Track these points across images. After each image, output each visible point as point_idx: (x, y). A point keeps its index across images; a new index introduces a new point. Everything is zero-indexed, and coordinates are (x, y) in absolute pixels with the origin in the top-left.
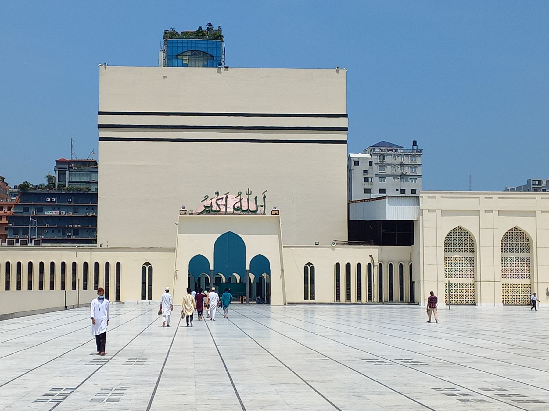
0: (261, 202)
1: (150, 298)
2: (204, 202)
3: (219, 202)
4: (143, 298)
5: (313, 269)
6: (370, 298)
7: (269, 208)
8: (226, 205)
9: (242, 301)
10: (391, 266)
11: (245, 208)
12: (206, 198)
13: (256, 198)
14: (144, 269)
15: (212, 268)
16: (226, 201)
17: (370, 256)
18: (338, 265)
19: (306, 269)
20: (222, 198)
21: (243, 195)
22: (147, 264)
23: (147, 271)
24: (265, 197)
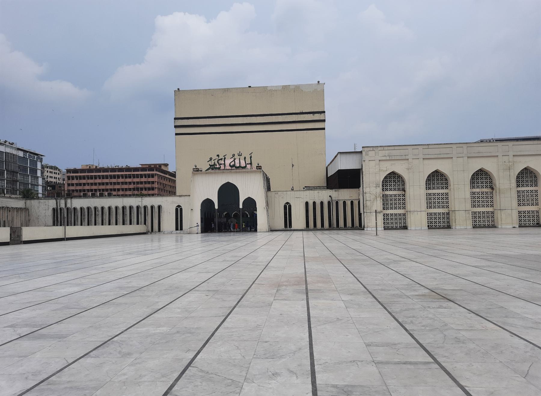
0: (248, 161)
1: (181, 229)
2: (210, 163)
3: (221, 162)
4: (177, 229)
5: (290, 206)
6: (330, 225)
7: (255, 165)
8: (225, 164)
9: (251, 229)
10: (344, 203)
11: (238, 165)
12: (211, 159)
13: (245, 158)
14: (177, 210)
15: (216, 207)
16: (224, 161)
17: (330, 196)
18: (307, 203)
19: (285, 207)
20: (222, 159)
21: (236, 156)
22: (179, 206)
23: (179, 211)
24: (251, 157)
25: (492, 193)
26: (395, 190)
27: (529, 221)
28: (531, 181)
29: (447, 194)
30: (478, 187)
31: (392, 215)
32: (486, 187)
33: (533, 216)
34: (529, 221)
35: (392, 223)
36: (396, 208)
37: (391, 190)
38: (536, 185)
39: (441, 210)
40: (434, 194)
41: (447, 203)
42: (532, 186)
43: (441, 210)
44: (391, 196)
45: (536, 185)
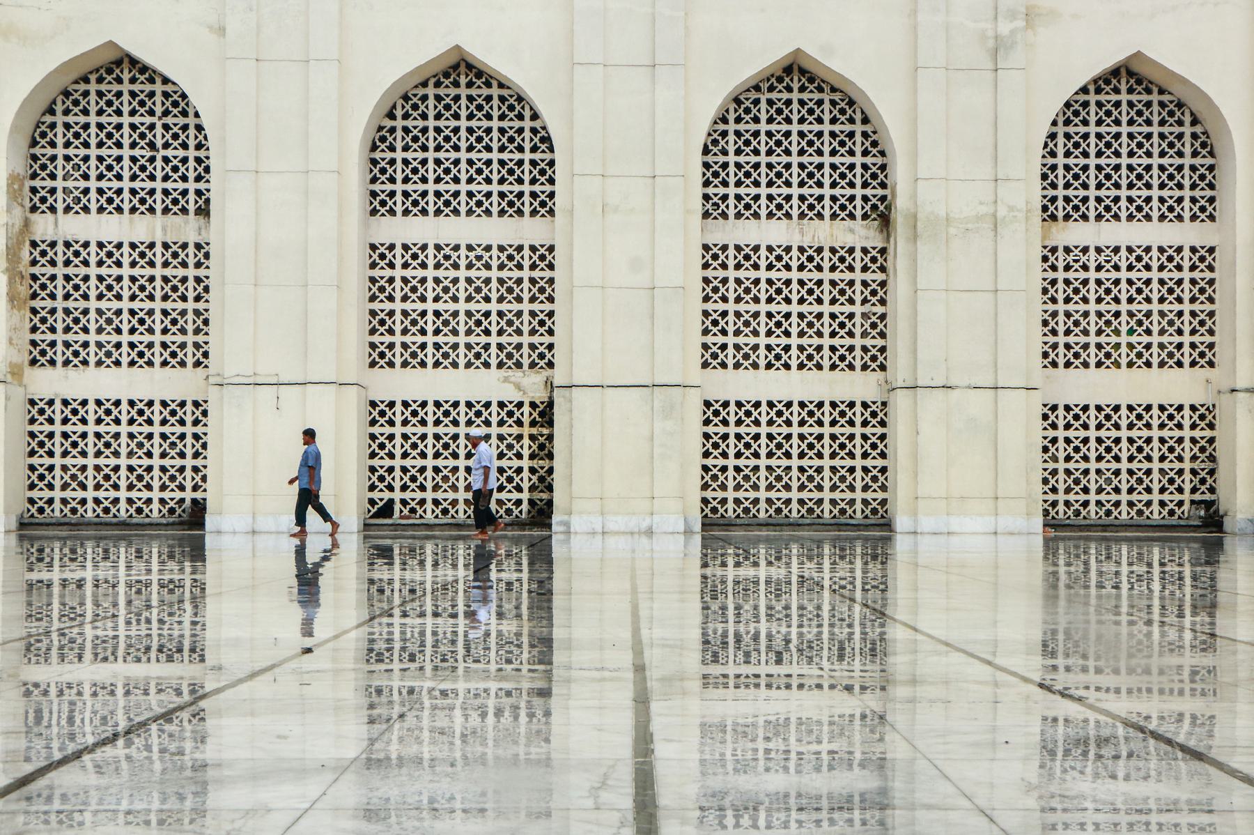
25: (879, 258)
26: (143, 204)
27: (1140, 481)
28: (1171, 177)
29: (544, 256)
30: (779, 210)
31: (107, 409)
32: (843, 211)
33: (1171, 449)
34: (1140, 481)
35: (108, 478)
36: (140, 358)
37: (110, 204)
38: (1206, 211)
39: (489, 385)
40: (446, 254)
41: (545, 323)
42: (1171, 213)
43: (489, 385)
44: (110, 252)
45: (1206, 211)
